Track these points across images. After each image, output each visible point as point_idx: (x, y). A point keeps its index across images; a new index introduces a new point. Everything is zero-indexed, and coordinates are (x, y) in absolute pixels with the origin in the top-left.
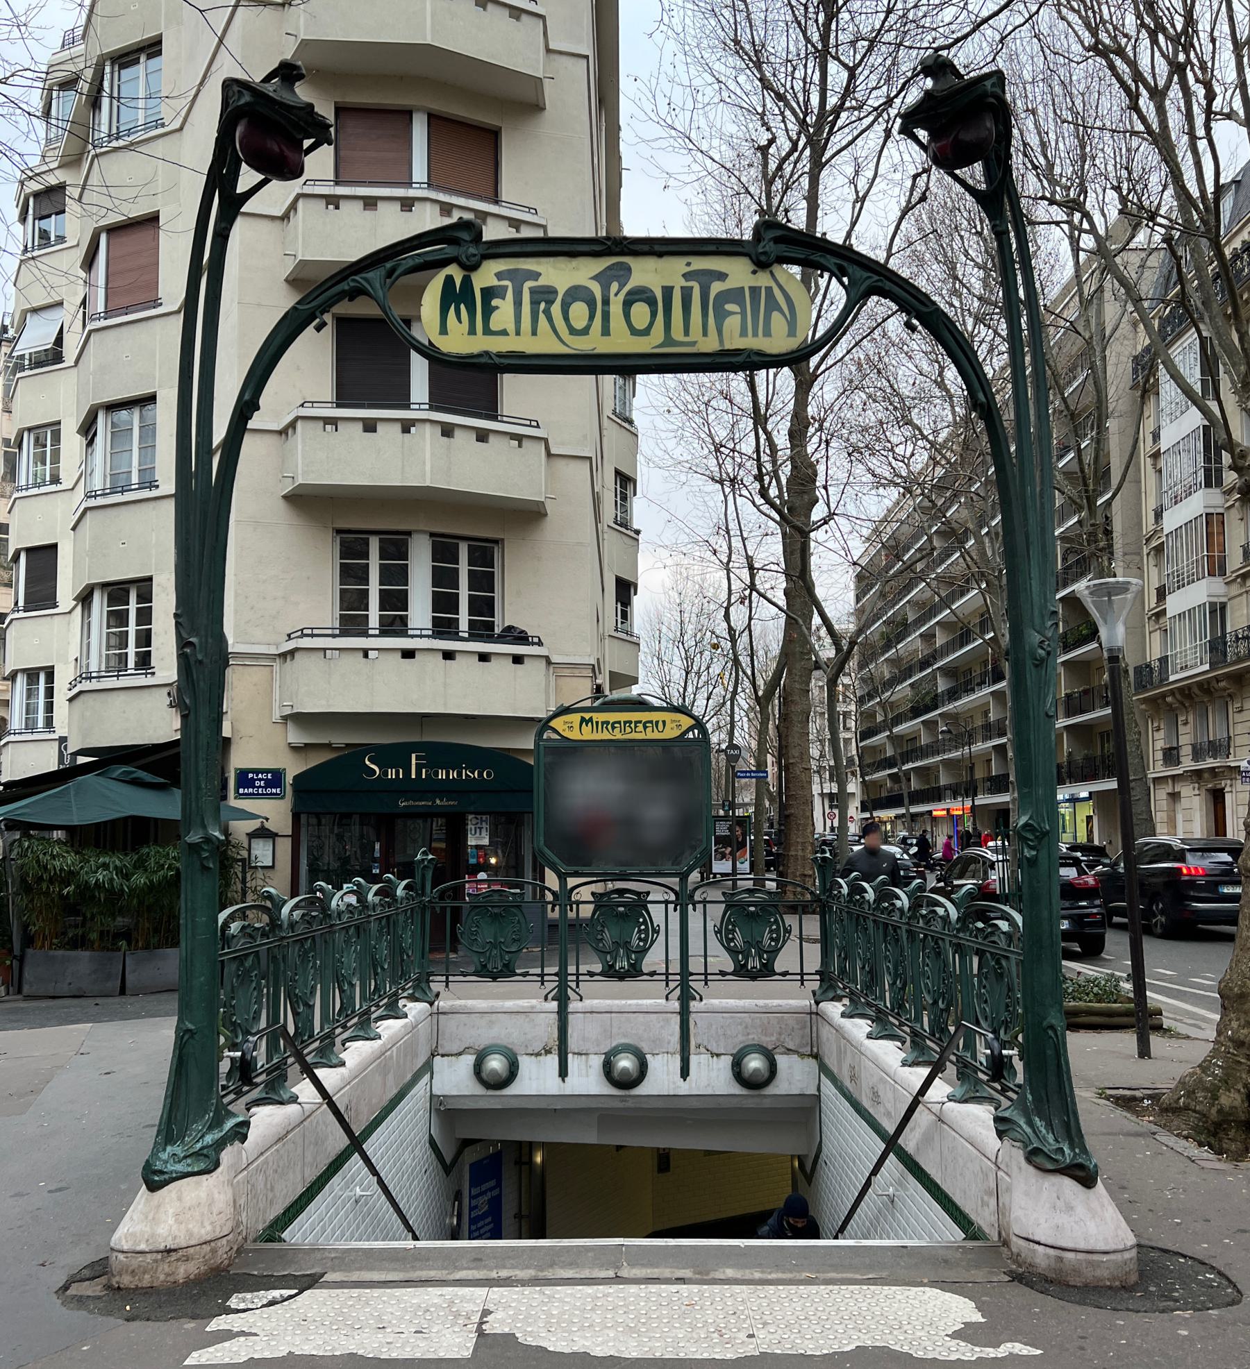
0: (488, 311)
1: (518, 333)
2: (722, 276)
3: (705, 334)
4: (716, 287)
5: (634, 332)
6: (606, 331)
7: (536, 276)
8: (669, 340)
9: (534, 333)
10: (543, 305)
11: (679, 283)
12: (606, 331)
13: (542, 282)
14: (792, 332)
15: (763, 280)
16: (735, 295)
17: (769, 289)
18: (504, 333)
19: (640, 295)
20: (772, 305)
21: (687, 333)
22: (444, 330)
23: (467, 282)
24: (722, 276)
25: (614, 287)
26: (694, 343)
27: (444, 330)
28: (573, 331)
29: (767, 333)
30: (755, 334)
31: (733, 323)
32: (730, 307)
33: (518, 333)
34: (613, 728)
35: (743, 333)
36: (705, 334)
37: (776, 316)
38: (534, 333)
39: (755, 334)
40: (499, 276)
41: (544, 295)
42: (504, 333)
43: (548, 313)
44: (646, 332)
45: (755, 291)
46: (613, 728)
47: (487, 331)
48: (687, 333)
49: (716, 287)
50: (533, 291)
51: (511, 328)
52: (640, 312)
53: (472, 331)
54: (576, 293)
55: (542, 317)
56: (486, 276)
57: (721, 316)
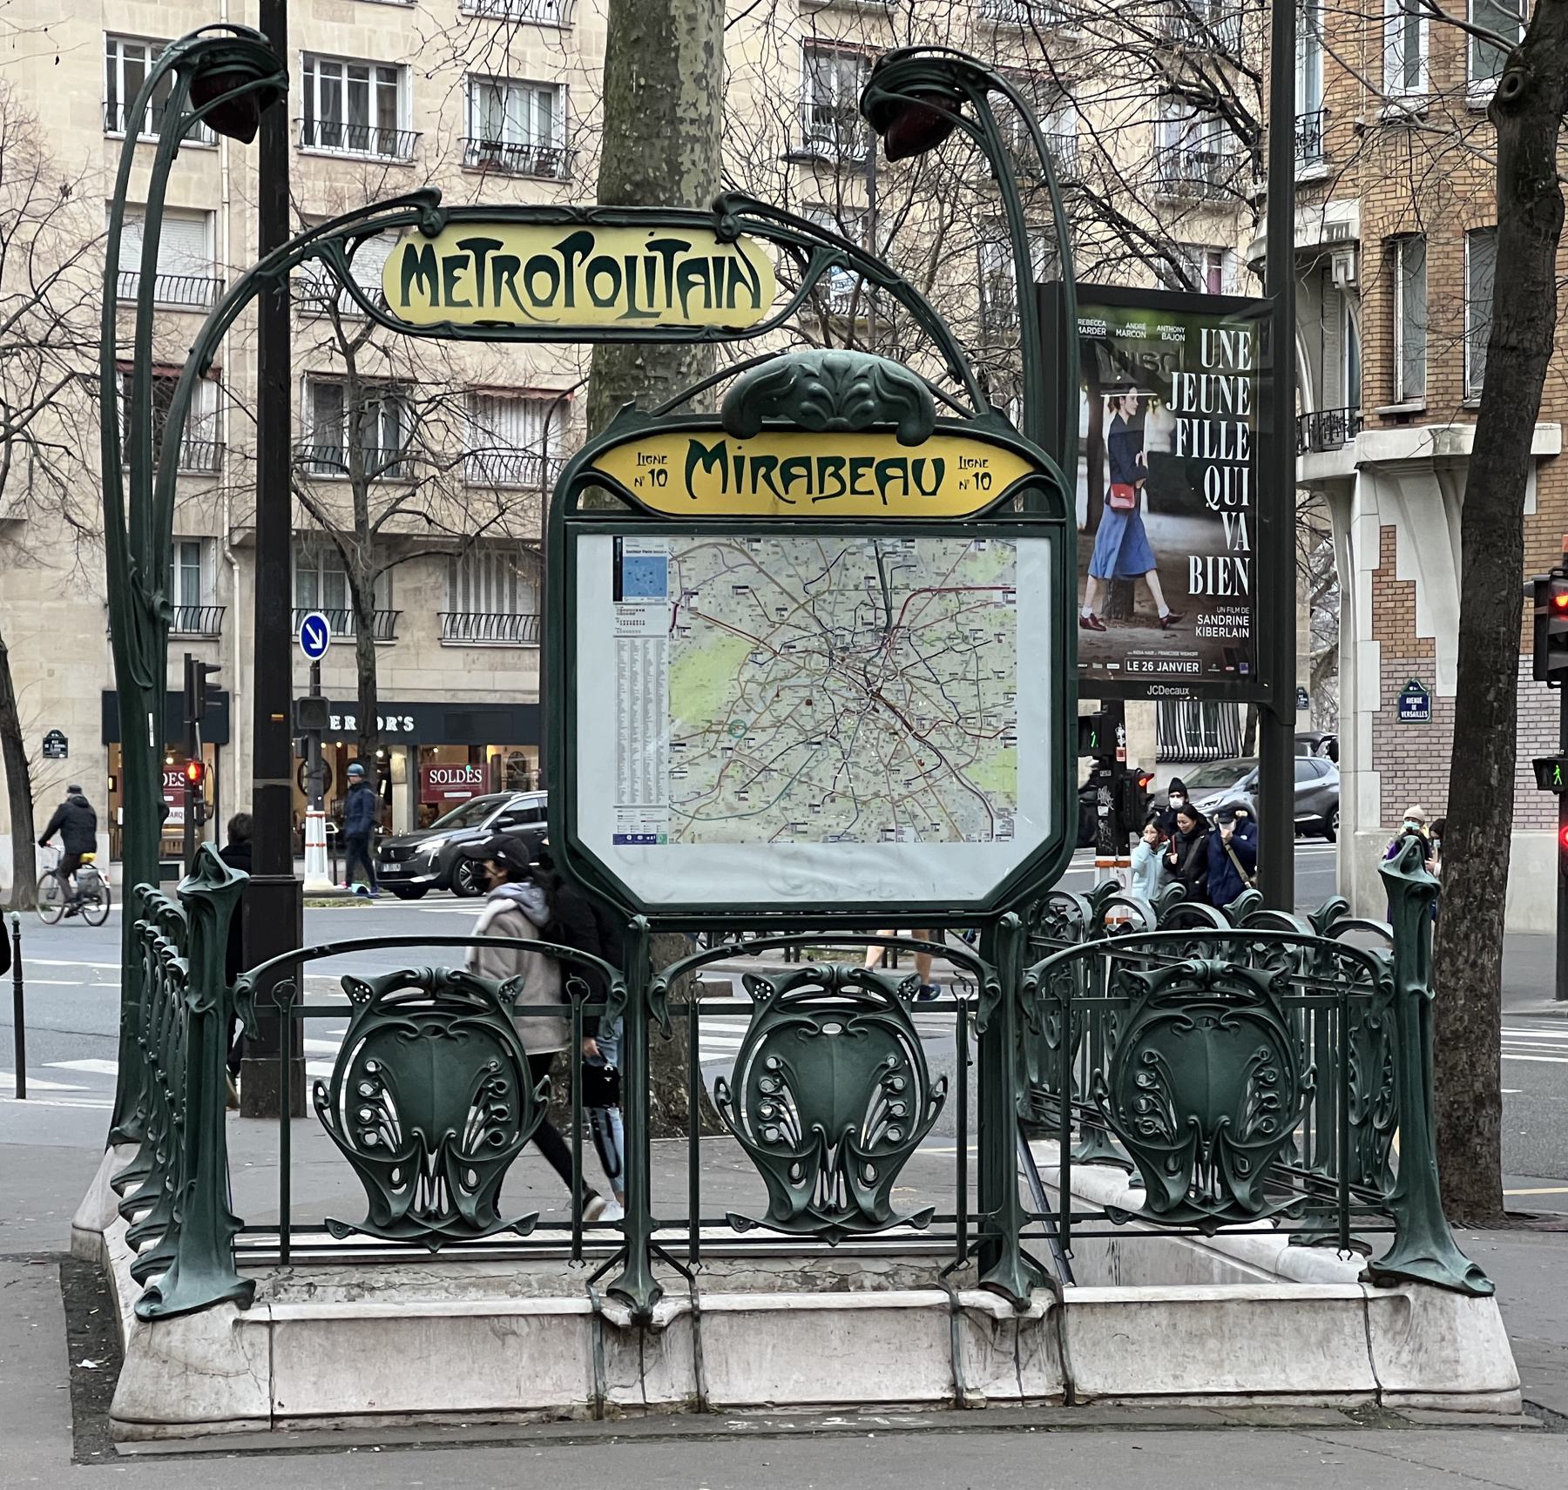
0: (451, 281)
1: (481, 304)
2: (685, 247)
3: (669, 305)
4: (680, 258)
5: (598, 303)
6: (570, 302)
7: (498, 245)
8: (633, 312)
9: (497, 303)
10: (505, 275)
11: (642, 253)
12: (570, 302)
13: (502, 252)
14: (756, 303)
15: (727, 252)
16: (699, 265)
17: (732, 260)
18: (467, 304)
19: (606, 264)
20: (736, 276)
21: (651, 304)
22: (405, 302)
23: (428, 250)
24: (685, 247)
25: (578, 256)
26: (657, 315)
27: (405, 302)
28: (536, 302)
29: (731, 304)
30: (719, 305)
31: (696, 295)
32: (692, 278)
33: (481, 304)
34: (788, 479)
35: (708, 304)
36: (669, 305)
37: (739, 285)
38: (497, 303)
39: (719, 305)
40: (462, 245)
41: (507, 264)
42: (467, 304)
43: (510, 283)
44: (610, 303)
45: (719, 262)
46: (788, 479)
47: (450, 302)
48: (651, 304)
49: (680, 258)
50: (493, 259)
51: (474, 301)
52: (604, 281)
53: (434, 302)
54: (541, 263)
55: (504, 286)
56: (447, 246)
57: (685, 286)
